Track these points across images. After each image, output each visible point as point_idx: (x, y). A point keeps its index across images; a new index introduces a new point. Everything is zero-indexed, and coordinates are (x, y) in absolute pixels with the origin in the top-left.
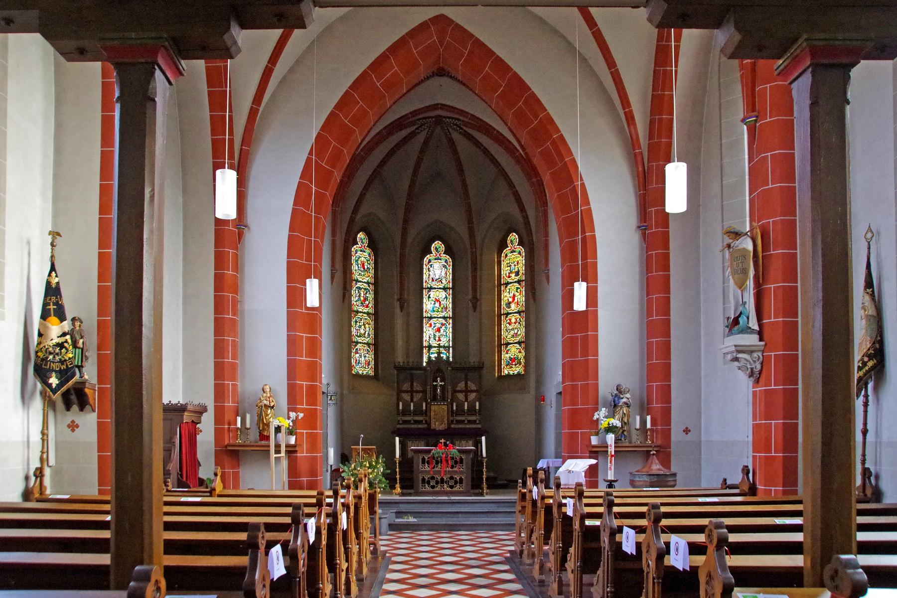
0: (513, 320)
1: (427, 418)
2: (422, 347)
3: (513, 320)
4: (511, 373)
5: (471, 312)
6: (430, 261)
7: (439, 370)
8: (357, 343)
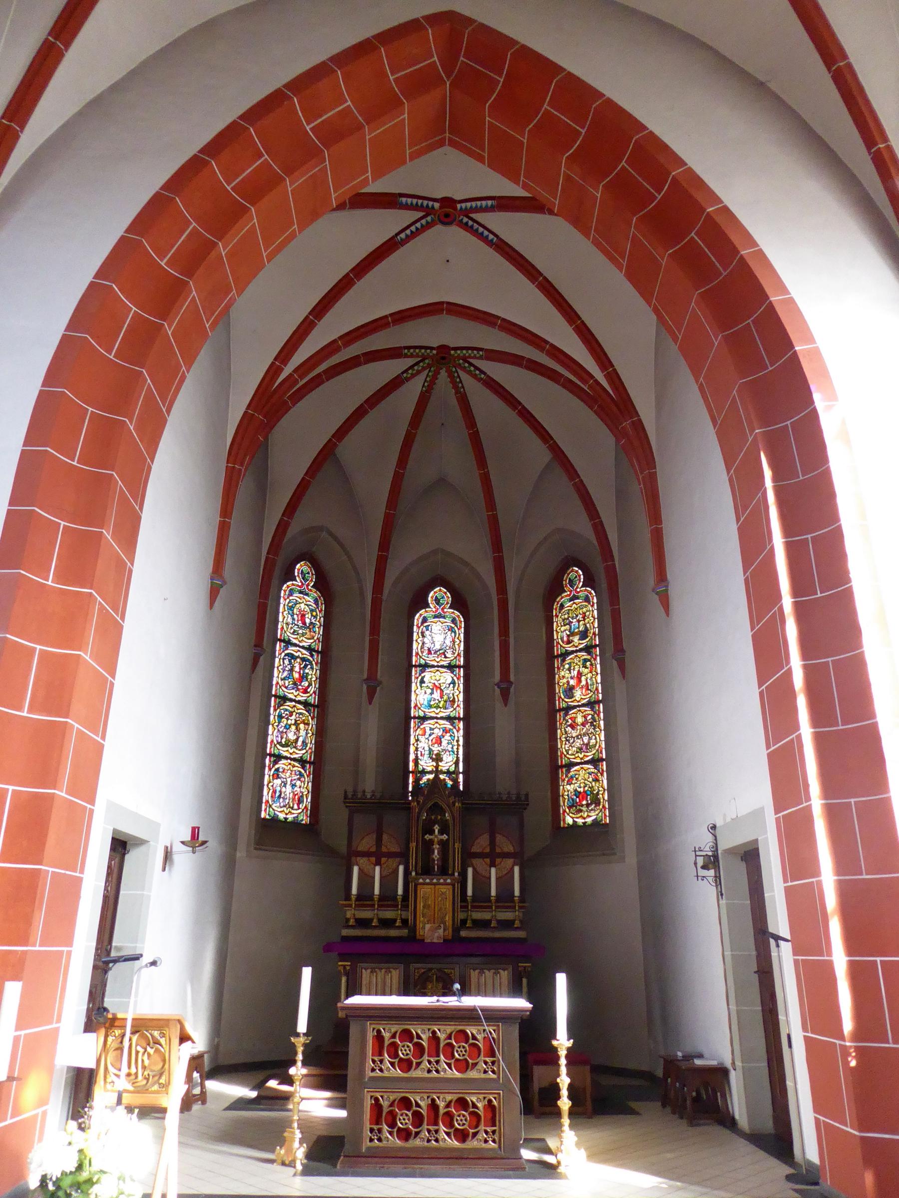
0: (580, 720)
2: (406, 772)
3: (580, 720)
4: (580, 821)
5: (499, 704)
6: (425, 620)
7: (436, 809)
8: (278, 758)
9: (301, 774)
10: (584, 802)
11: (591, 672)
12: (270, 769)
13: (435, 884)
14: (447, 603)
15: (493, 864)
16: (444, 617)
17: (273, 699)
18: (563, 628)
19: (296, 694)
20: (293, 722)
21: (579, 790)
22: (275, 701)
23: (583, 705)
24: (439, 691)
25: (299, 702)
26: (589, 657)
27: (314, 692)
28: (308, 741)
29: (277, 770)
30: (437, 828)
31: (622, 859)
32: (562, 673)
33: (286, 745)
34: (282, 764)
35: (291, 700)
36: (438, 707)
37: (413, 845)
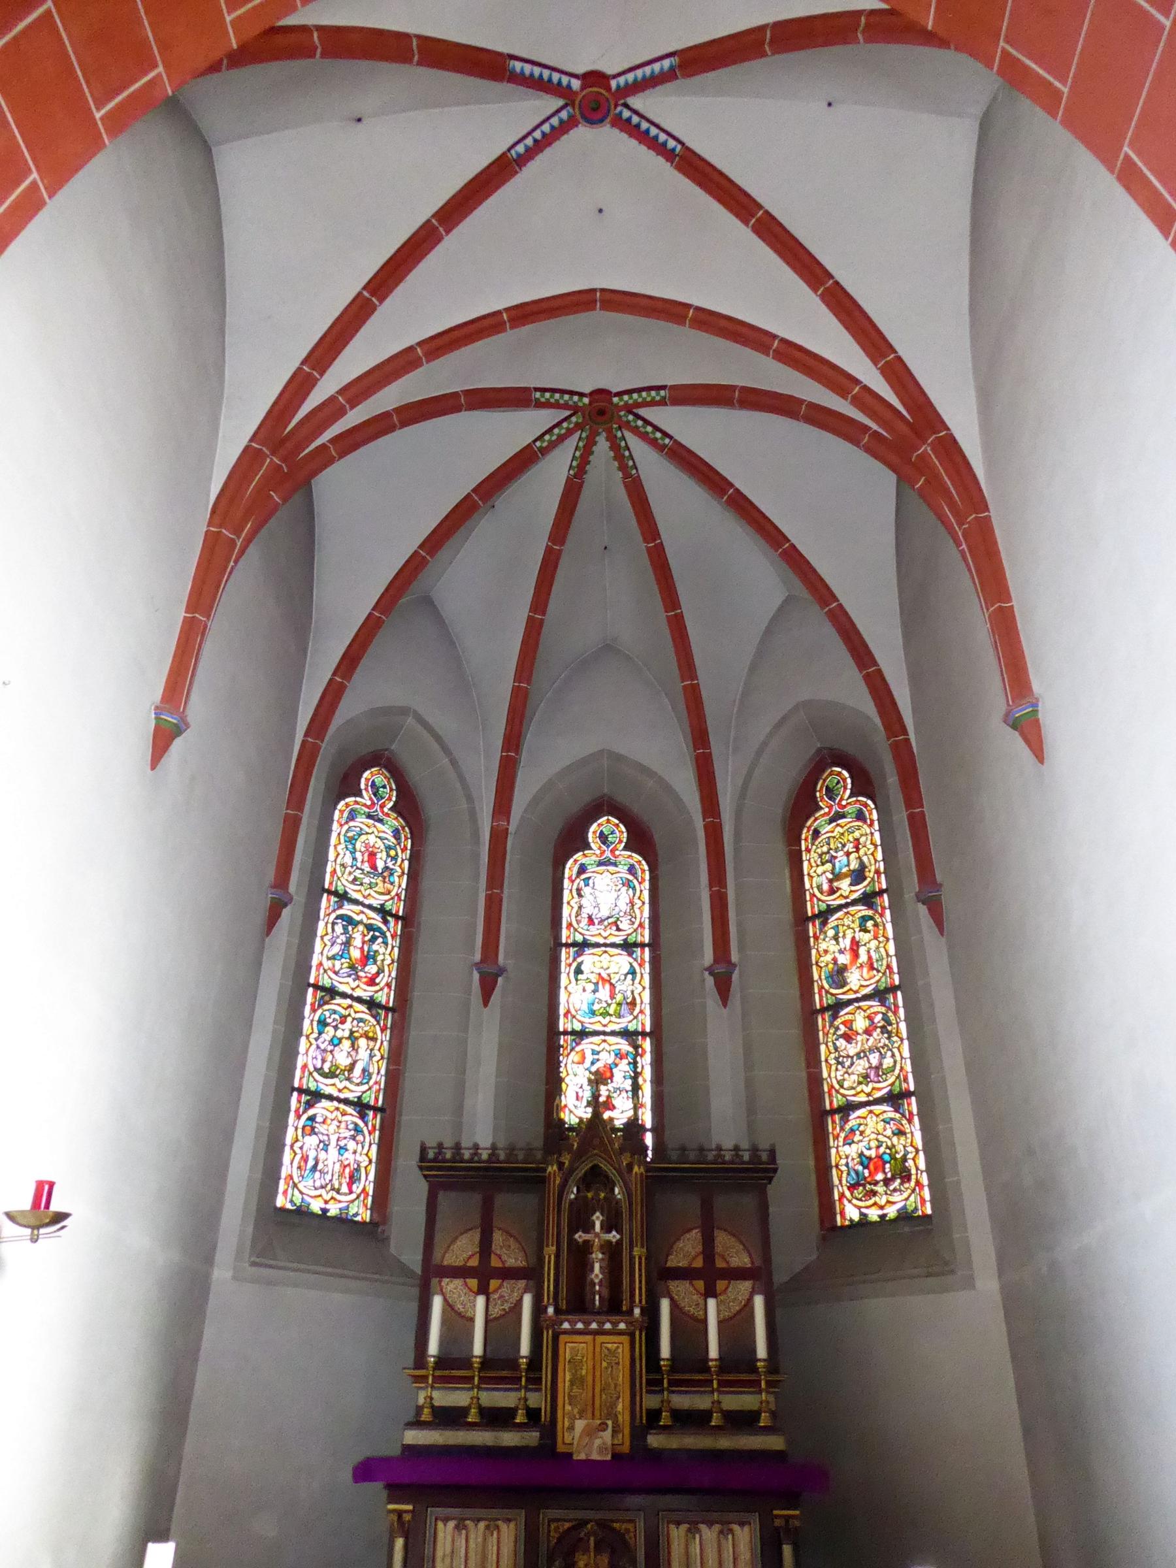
0: (860, 1024)
1: (536, 1400)
3: (860, 1024)
4: (874, 1215)
6: (582, 869)
7: (595, 1178)
8: (316, 1096)
9: (357, 1129)
10: (880, 1177)
11: (876, 938)
12: (299, 1117)
13: (595, 1333)
14: (620, 842)
15: (710, 1292)
16: (615, 865)
17: (311, 990)
18: (820, 870)
19: (354, 985)
20: (347, 1034)
21: (867, 1153)
22: (314, 995)
23: (866, 998)
24: (607, 986)
25: (359, 1000)
26: (870, 913)
27: (388, 985)
28: (373, 1069)
29: (312, 1118)
30: (598, 1219)
31: (969, 1282)
32: (823, 946)
33: (332, 1075)
34: (322, 1109)
35: (344, 995)
36: (605, 1014)
37: (550, 1250)
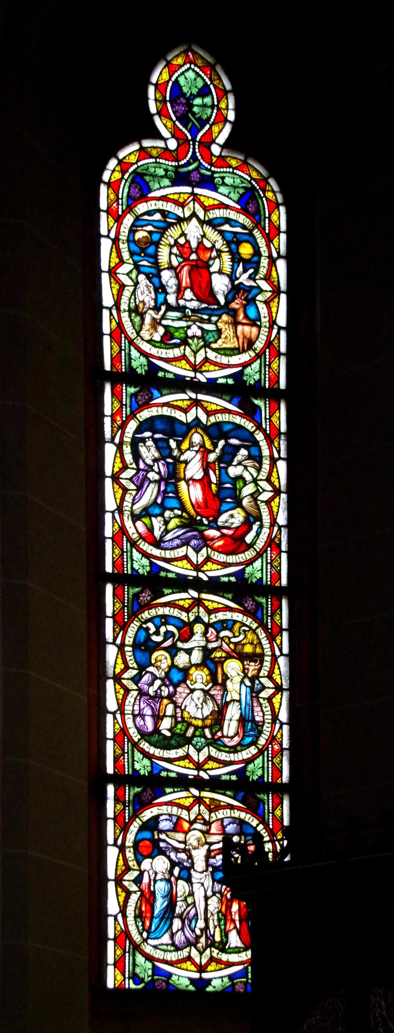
20: (197, 657)
25: (214, 586)
27: (272, 543)
33: (178, 739)
34: (166, 807)
35: (181, 583)
